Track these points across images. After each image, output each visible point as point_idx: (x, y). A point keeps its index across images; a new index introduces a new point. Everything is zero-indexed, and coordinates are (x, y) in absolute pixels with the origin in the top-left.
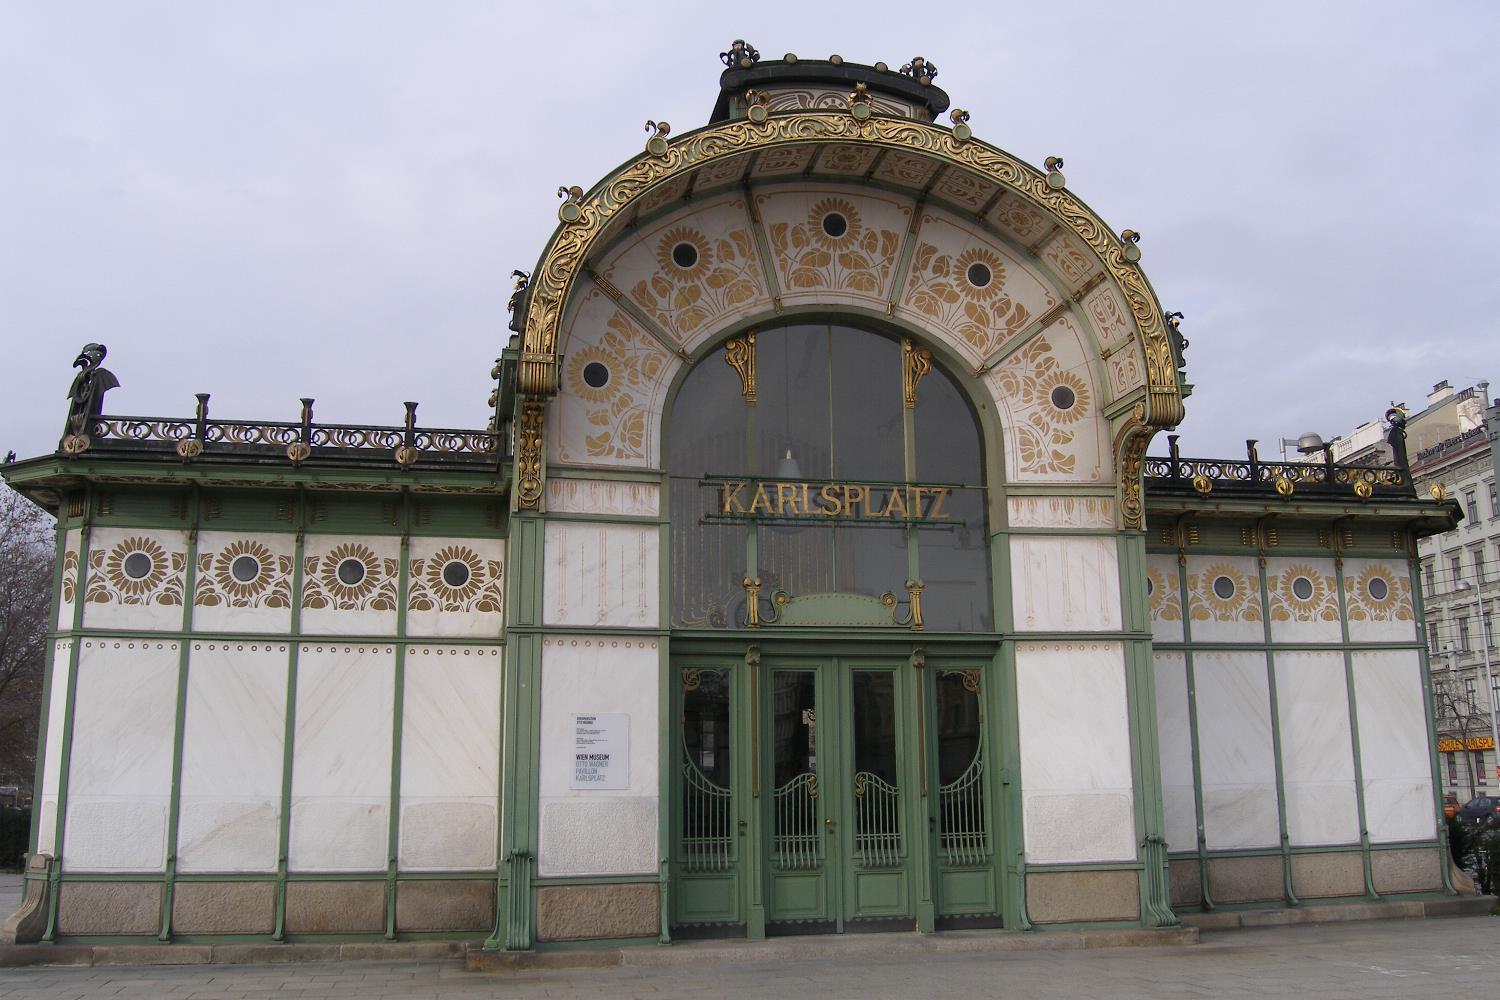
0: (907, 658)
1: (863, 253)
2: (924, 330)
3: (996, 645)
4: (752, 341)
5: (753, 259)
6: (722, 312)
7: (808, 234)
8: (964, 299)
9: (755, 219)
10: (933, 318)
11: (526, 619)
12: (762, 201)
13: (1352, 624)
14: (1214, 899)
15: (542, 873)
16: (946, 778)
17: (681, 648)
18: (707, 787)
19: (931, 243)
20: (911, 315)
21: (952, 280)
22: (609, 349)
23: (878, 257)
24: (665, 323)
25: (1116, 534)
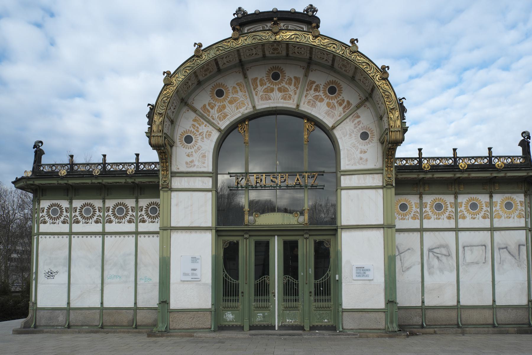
0: (303, 235)
1: (287, 86)
2: (310, 114)
3: (336, 230)
4: (247, 123)
5: (245, 92)
6: (234, 113)
7: (266, 81)
8: (326, 100)
9: (245, 77)
10: (314, 109)
11: (165, 225)
12: (248, 70)
13: (495, 220)
14: (427, 323)
15: (171, 308)
16: (316, 277)
17: (219, 233)
18: (231, 280)
19: (313, 80)
20: (305, 108)
21: (321, 93)
22: (193, 130)
23: (292, 87)
24: (213, 119)
25: (382, 187)
